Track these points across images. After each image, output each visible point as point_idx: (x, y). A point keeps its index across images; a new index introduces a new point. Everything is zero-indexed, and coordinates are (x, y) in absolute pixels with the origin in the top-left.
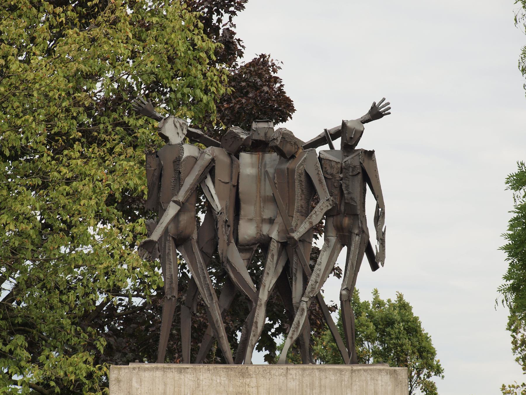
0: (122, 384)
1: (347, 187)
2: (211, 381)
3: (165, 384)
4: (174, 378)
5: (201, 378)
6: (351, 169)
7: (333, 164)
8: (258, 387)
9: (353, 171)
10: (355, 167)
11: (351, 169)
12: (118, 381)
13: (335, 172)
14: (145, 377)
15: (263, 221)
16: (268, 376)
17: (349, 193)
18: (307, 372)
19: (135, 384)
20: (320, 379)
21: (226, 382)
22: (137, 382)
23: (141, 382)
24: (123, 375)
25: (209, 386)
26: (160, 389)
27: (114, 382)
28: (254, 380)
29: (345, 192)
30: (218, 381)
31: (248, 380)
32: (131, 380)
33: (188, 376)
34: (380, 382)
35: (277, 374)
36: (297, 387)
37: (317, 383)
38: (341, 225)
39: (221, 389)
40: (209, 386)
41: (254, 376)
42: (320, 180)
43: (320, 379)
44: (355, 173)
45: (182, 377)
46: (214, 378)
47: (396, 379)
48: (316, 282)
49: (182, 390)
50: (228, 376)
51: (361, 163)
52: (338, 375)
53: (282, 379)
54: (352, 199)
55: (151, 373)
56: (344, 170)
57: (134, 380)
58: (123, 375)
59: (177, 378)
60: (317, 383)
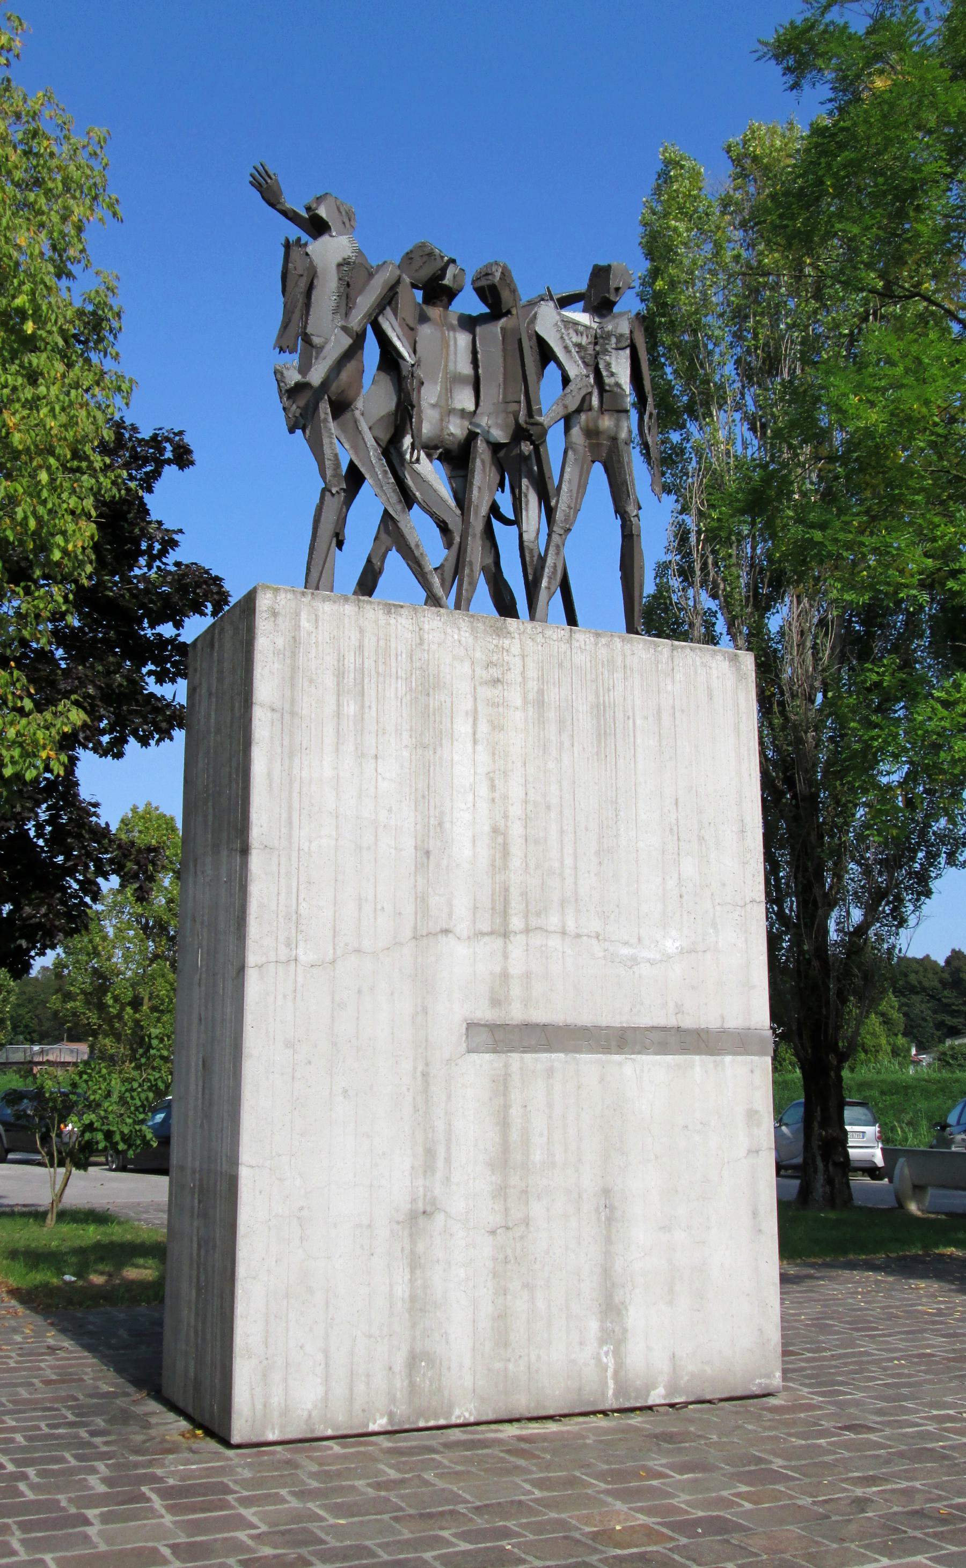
0: (280, 620)
1: (608, 365)
2: (442, 636)
3: (361, 631)
4: (376, 622)
5: (426, 627)
6: (613, 340)
7: (580, 328)
8: (523, 657)
9: (618, 341)
10: (621, 335)
11: (613, 340)
12: (275, 614)
13: (584, 341)
14: (324, 613)
15: (451, 411)
16: (539, 639)
17: (612, 374)
18: (603, 641)
19: (305, 624)
20: (624, 656)
21: (470, 640)
22: (308, 621)
23: (317, 621)
24: (283, 602)
25: (439, 644)
26: (353, 638)
27: (265, 615)
28: (517, 641)
29: (604, 373)
30: (456, 637)
31: (507, 642)
32: (298, 614)
33: (403, 620)
34: (715, 673)
35: (555, 637)
36: (588, 665)
37: (619, 659)
38: (597, 427)
39: (462, 652)
40: (439, 644)
41: (517, 636)
42: (566, 348)
43: (624, 656)
44: (621, 345)
45: (393, 621)
46: (449, 630)
47: (738, 669)
48: (570, 507)
49: (393, 645)
50: (473, 630)
51: (631, 332)
52: (652, 651)
53: (564, 647)
54: (618, 385)
55: (336, 607)
56: (601, 341)
57: (304, 616)
58: (283, 602)
59: (382, 622)
60: (619, 659)
